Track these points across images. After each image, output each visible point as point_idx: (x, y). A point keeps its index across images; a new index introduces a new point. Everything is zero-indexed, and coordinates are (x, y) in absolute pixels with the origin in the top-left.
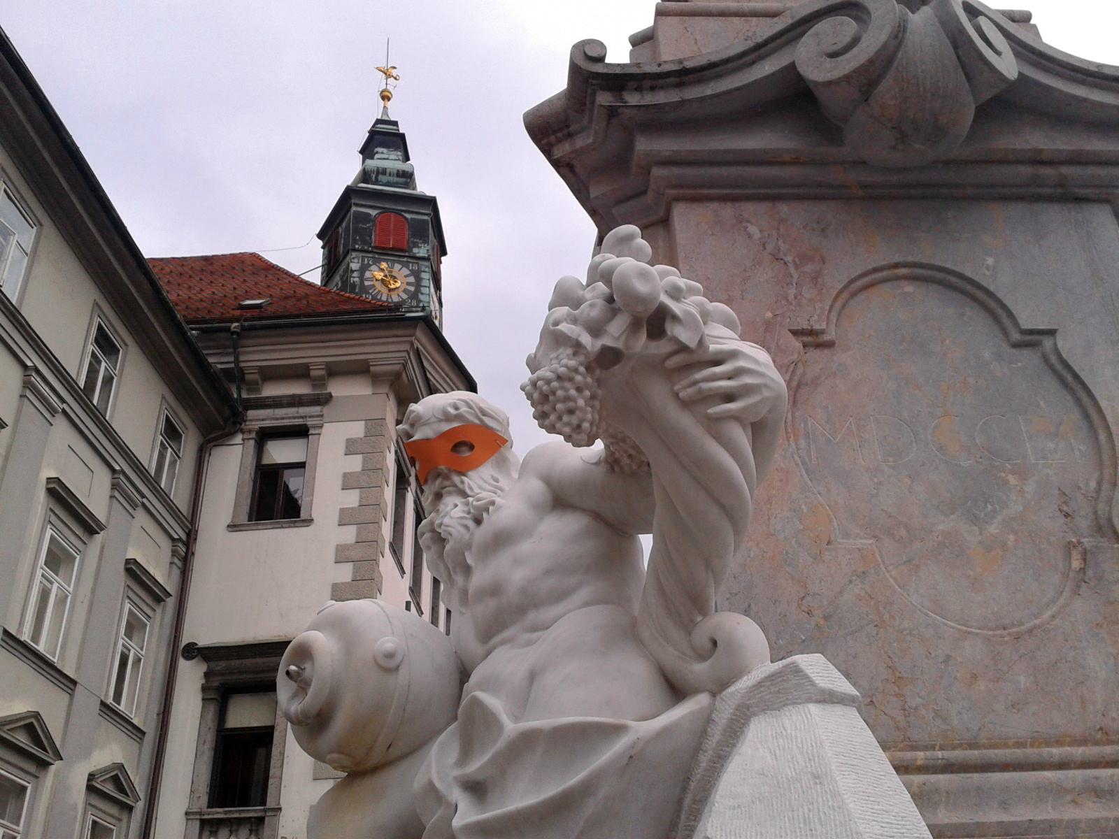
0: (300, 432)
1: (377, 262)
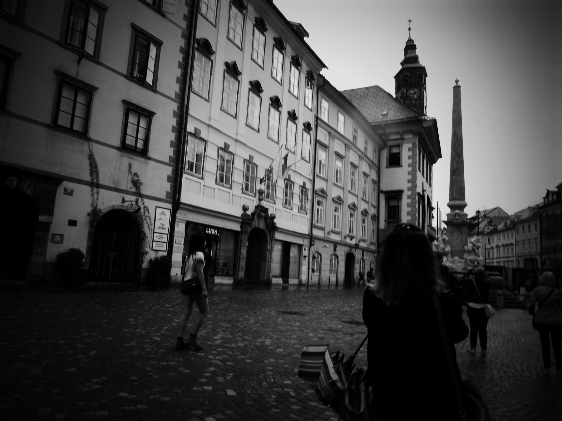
1: (410, 89)
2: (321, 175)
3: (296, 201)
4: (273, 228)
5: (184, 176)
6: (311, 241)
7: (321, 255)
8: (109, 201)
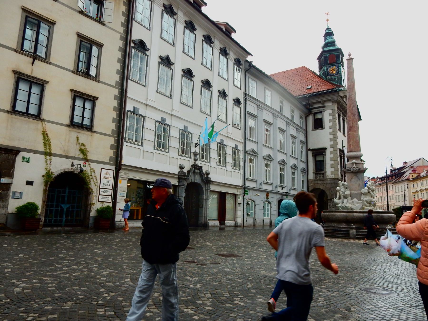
0: (321, 112)
1: (330, 67)
2: (252, 139)
3: (229, 159)
4: (208, 182)
5: (125, 144)
6: (245, 191)
7: (254, 202)
8: (59, 166)
